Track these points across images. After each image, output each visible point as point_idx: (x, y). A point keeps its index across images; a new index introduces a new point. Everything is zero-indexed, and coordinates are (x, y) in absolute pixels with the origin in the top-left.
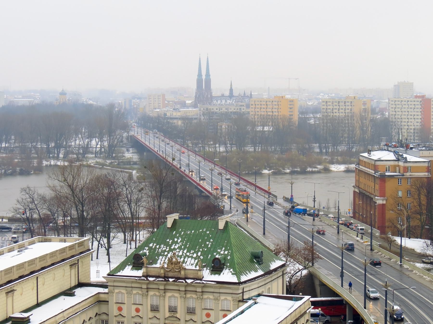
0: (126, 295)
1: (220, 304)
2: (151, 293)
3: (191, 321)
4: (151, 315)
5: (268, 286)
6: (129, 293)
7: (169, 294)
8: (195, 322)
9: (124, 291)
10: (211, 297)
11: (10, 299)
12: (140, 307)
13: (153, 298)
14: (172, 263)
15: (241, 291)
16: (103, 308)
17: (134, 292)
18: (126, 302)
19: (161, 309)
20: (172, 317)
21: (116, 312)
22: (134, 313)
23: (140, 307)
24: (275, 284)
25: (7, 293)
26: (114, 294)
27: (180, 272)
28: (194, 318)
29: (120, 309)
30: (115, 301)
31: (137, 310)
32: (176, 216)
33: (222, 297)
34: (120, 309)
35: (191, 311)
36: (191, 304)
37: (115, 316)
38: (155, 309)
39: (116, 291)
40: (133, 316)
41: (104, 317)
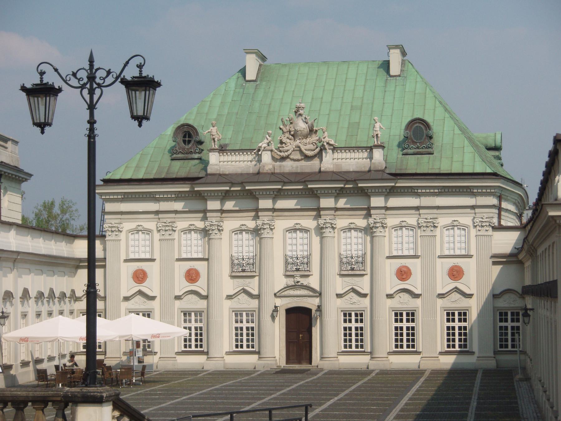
0: (157, 236)
1: (438, 238)
3: (352, 294)
8: (365, 296)
9: (151, 225)
10: (412, 220)
14: (292, 135)
17: (182, 224)
18: (156, 256)
20: (296, 286)
22: (181, 285)
23: (201, 267)
26: (123, 236)
27: (319, 155)
29: (140, 277)
30: (123, 257)
33: (444, 220)
34: (140, 277)
36: (353, 244)
37: (126, 299)
39: (128, 225)
40: (178, 293)
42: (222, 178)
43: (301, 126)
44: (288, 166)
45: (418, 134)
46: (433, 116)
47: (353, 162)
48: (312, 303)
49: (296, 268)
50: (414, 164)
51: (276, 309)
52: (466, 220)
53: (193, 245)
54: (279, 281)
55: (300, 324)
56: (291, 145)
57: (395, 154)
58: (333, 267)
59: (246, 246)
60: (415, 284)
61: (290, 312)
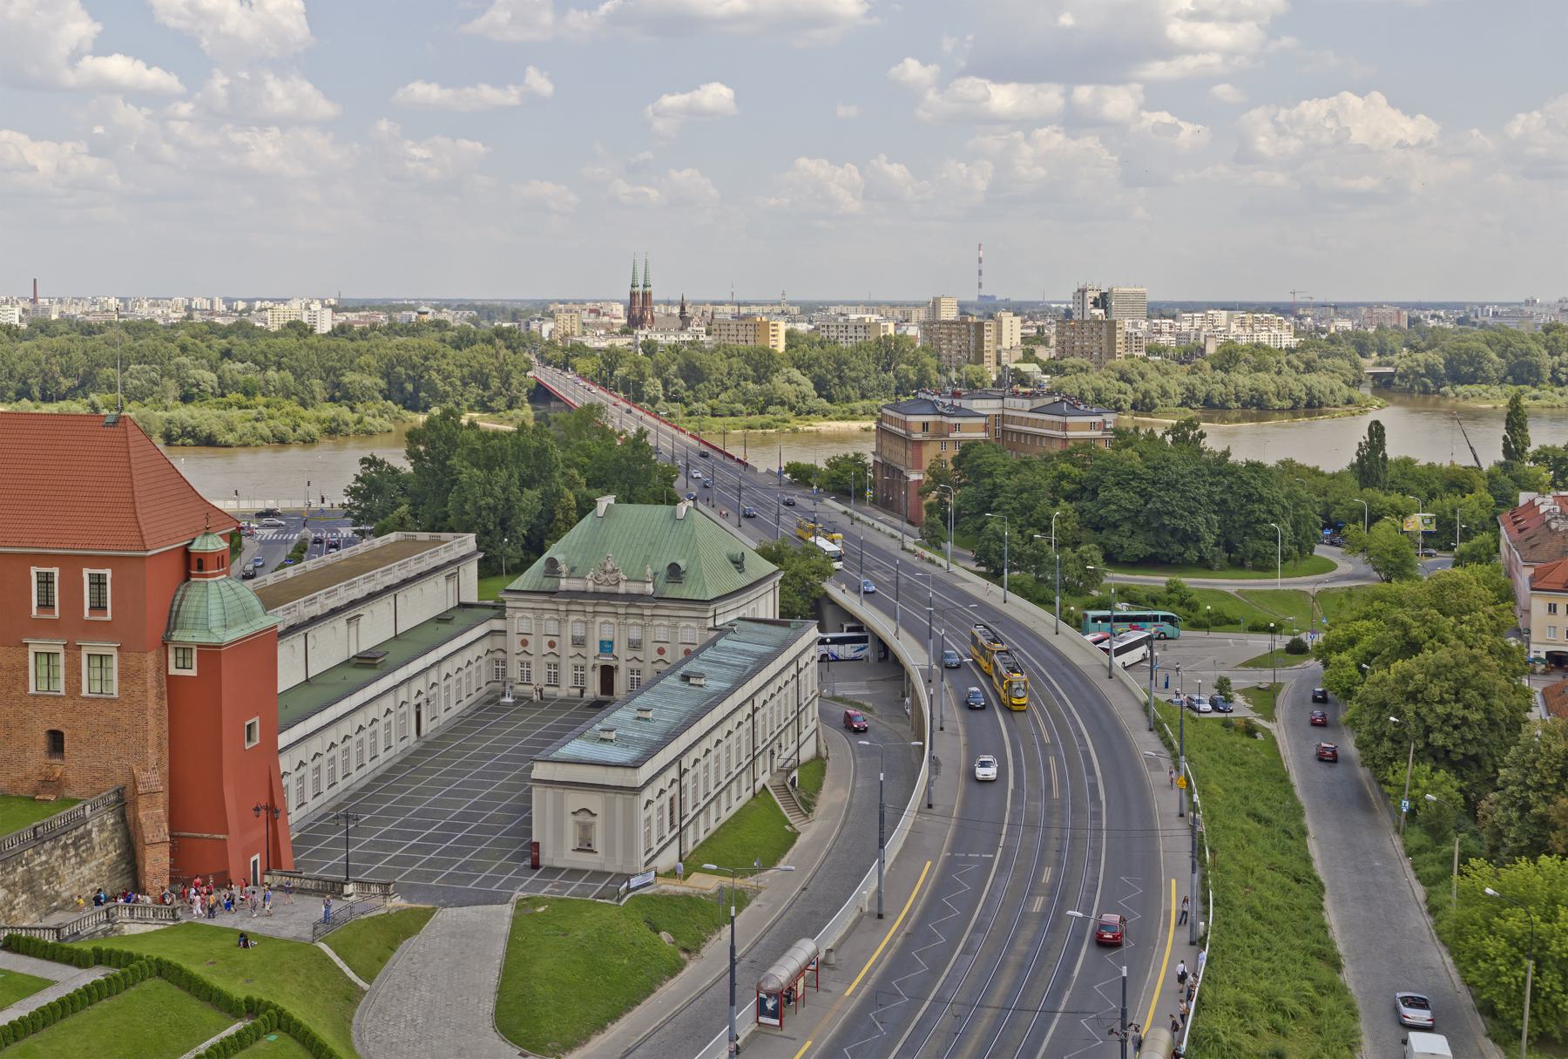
2: (572, 618)
4: (572, 651)
5: (752, 606)
6: (539, 618)
7: (600, 619)
9: (530, 615)
11: (353, 629)
12: (555, 639)
13: (574, 627)
15: (711, 614)
16: (498, 642)
17: (547, 616)
19: (590, 642)
21: (518, 648)
22: (546, 650)
24: (762, 602)
25: (349, 621)
28: (640, 655)
29: (524, 643)
31: (552, 644)
32: (610, 499)
33: (683, 624)
34: (524, 643)
35: (635, 645)
36: (635, 634)
38: (579, 642)
39: (519, 615)
41: (500, 655)
42: (569, 593)
43: (609, 567)
44: (603, 589)
45: (675, 572)
46: (682, 563)
47: (635, 588)
48: (613, 664)
49: (606, 646)
50: (673, 591)
51: (594, 667)
52: (693, 624)
53: (552, 628)
54: (597, 652)
55: (607, 674)
56: (603, 577)
57: (661, 582)
58: (624, 645)
59: (579, 631)
60: (667, 657)
61: (603, 667)
